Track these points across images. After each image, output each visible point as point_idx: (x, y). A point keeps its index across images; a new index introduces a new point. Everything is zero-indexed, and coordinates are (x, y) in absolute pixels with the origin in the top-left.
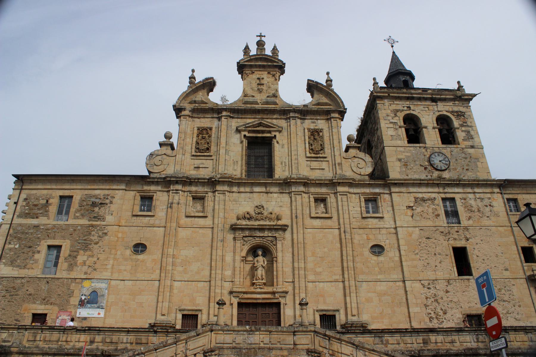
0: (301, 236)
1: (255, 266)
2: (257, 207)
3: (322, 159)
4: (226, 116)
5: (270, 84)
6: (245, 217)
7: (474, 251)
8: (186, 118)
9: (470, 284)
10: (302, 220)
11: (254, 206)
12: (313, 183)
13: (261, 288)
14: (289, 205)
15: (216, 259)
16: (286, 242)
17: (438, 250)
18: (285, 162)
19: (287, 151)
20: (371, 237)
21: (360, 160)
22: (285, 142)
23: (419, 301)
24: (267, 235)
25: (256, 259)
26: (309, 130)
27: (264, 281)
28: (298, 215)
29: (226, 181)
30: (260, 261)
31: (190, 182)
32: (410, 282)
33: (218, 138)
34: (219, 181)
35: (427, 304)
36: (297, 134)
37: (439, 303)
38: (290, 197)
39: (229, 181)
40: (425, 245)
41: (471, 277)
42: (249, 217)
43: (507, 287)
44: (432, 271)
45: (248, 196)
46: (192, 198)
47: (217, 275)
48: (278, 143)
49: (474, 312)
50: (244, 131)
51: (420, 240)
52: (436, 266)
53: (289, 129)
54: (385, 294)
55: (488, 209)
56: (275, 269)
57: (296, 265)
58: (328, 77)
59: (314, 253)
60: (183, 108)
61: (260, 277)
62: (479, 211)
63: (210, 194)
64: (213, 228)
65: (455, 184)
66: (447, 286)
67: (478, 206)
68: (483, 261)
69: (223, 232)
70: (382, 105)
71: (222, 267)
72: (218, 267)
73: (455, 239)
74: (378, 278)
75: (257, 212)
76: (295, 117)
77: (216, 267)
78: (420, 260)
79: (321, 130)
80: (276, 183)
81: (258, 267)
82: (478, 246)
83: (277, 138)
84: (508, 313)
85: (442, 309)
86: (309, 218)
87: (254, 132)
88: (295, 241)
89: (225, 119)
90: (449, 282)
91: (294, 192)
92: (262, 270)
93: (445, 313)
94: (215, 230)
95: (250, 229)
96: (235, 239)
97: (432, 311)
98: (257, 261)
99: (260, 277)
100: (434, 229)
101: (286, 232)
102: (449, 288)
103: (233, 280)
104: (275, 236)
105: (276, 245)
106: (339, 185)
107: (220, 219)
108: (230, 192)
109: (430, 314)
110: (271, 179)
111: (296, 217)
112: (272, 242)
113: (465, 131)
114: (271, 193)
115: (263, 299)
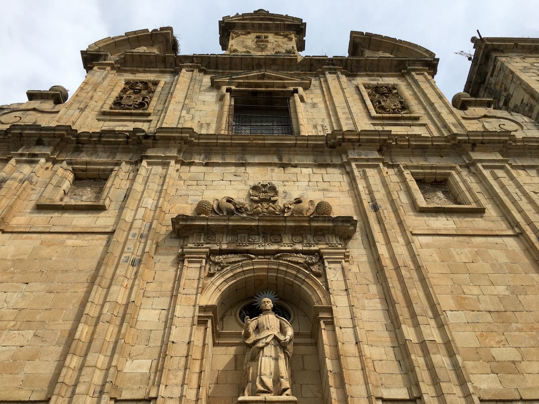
0: (400, 249)
1: (249, 341)
2: (255, 188)
3: (410, 122)
4: (191, 66)
5: (280, 43)
6: (219, 208)
8: (104, 69)
10: (392, 215)
11: (248, 188)
12: (402, 147)
14: (346, 187)
15: (99, 318)
16: (354, 269)
18: (322, 126)
19: (324, 111)
21: (502, 120)
22: (318, 100)
24: (289, 248)
25: (252, 324)
26: (367, 87)
27: (284, 397)
28: (379, 203)
29: (174, 138)
30: (267, 324)
31: (78, 142)
33: (170, 94)
36: (343, 89)
38: (348, 173)
39: (182, 138)
42: (233, 207)
45: (233, 171)
46: (71, 176)
47: (85, 371)
48: (302, 100)
50: (229, 83)
53: (323, 86)
56: (327, 349)
57: (409, 332)
59: (465, 298)
60: (101, 55)
61: (269, 382)
63: (125, 167)
64: (113, 232)
69: (143, 240)
70: (508, 58)
71: (116, 342)
72: (96, 344)
75: (256, 198)
76: (335, 69)
77: (91, 342)
79: (394, 87)
80: (307, 146)
81: (260, 345)
83: (299, 92)
86: (412, 213)
87: (249, 85)
88: (386, 261)
89: (187, 71)
91: (356, 160)
92: (276, 359)
94: (119, 237)
95: (234, 231)
96: (181, 259)
98: (257, 327)
99: (269, 382)
101: (350, 243)
103: (153, 394)
104: (318, 251)
105: (322, 275)
106: (473, 150)
107: (141, 211)
108: (183, 164)
110: (293, 138)
111: (375, 208)
112: (308, 266)
114: (295, 166)
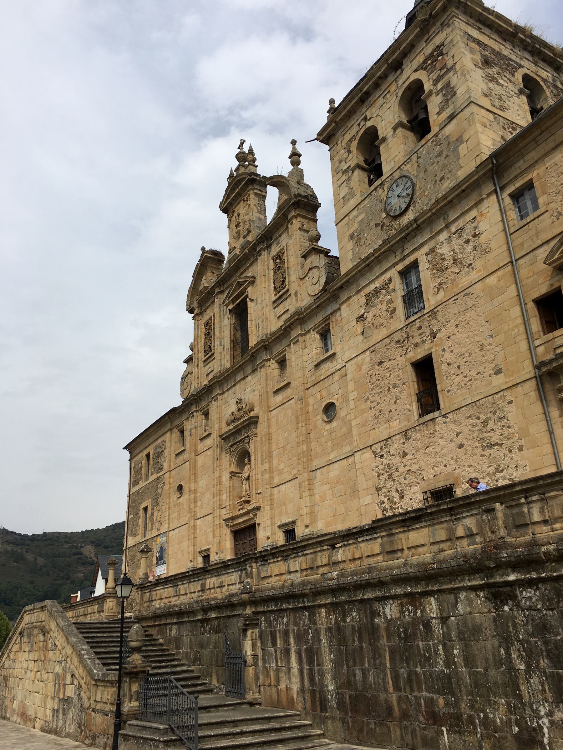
7: (443, 356)
9: (437, 428)
13: (242, 509)
17: (393, 380)
20: (324, 393)
23: (370, 483)
32: (360, 452)
34: (211, 386)
35: (379, 486)
37: (394, 480)
40: (377, 377)
41: (436, 414)
43: (498, 412)
44: (386, 423)
49: (440, 484)
51: (370, 373)
52: (390, 411)
54: (337, 482)
55: (469, 247)
58: (294, 148)
62: (455, 260)
65: (413, 230)
66: (404, 443)
67: (453, 250)
68: (457, 372)
73: (416, 345)
74: (331, 458)
78: (371, 409)
82: (450, 342)
84: (498, 471)
85: (397, 491)
90: (406, 436)
93: (401, 497)
97: (385, 496)
100: (388, 341)
102: (408, 448)
109: (383, 503)
113: (442, 90)
115: (244, 522)
